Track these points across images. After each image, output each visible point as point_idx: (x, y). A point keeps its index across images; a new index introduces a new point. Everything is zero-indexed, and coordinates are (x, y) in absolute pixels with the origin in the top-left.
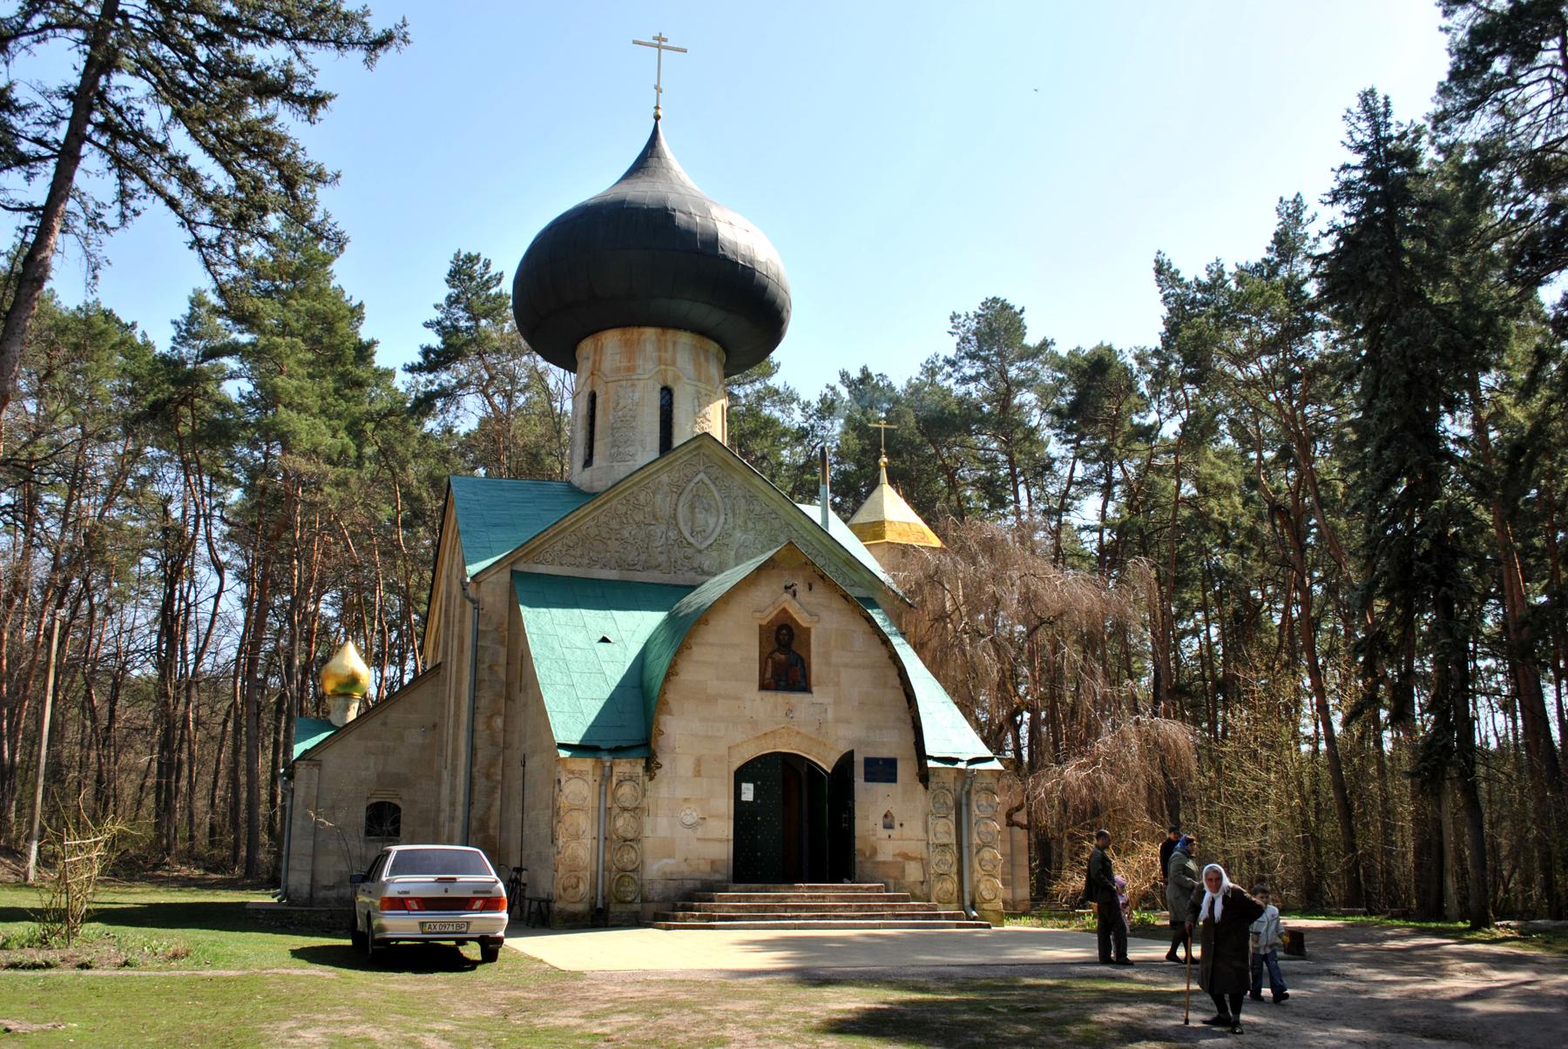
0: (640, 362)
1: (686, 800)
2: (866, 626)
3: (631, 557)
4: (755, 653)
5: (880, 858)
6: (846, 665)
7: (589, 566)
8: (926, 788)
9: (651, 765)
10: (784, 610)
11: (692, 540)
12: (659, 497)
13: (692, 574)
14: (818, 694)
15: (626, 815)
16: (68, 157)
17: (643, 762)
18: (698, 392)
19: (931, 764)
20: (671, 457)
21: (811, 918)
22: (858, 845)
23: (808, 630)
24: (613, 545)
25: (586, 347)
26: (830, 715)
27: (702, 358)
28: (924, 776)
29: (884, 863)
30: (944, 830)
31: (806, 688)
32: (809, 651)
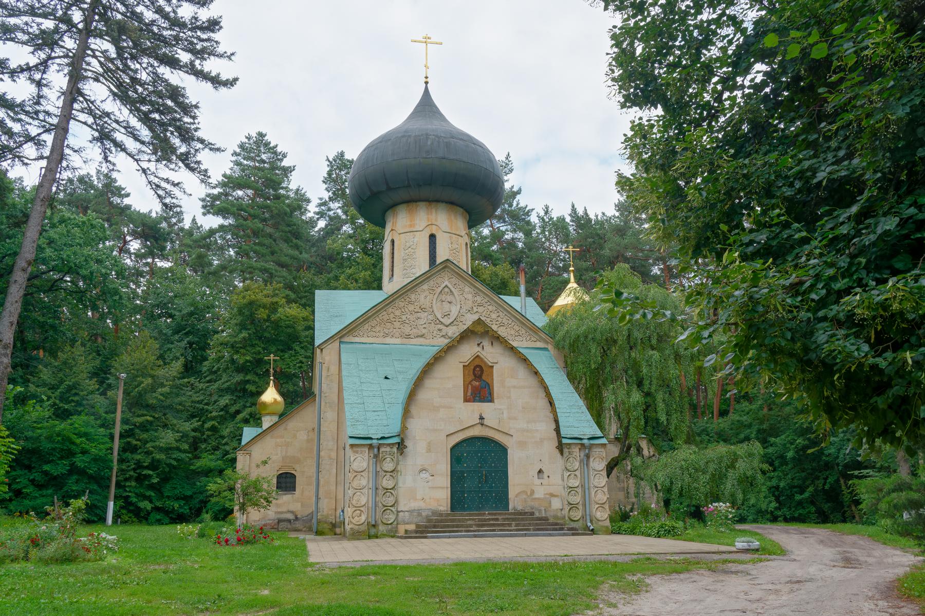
3: (407, 329)
4: (460, 382)
5: (536, 496)
6: (514, 387)
9: (401, 446)
12: (422, 297)
13: (442, 339)
14: (498, 404)
16: (61, 131)
19: (564, 441)
24: (397, 324)
26: (505, 415)
27: (453, 217)
29: (539, 499)
31: (491, 400)
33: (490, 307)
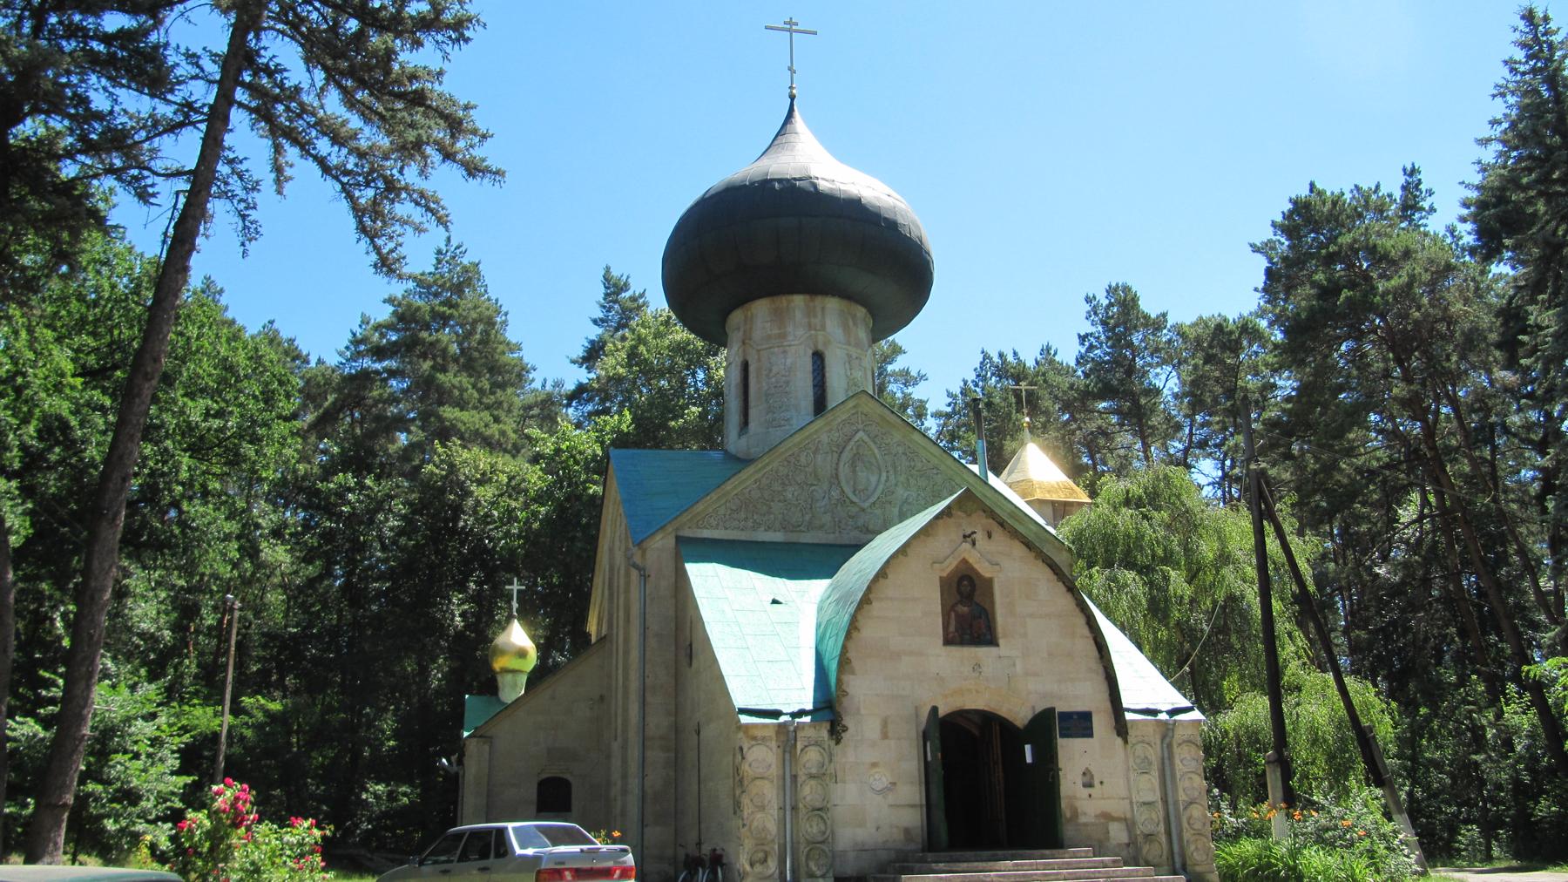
0: (790, 329)
1: (874, 765)
5: (1083, 819)
6: (1031, 616)
7: (754, 529)
8: (1126, 742)
9: (836, 729)
10: (964, 561)
11: (854, 499)
13: (856, 533)
14: (1005, 647)
15: (813, 782)
16: (217, 119)
17: (828, 726)
18: (849, 356)
20: (829, 416)
22: (1063, 805)
23: (990, 581)
25: (736, 317)
29: (1085, 825)
30: (1148, 788)
31: (992, 641)
32: (992, 603)
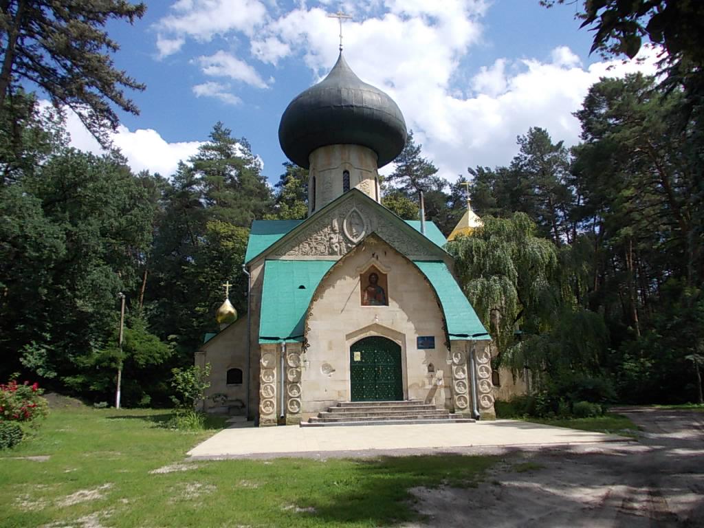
2: (416, 272)
3: (322, 248)
9: (304, 344)
10: (373, 266)
11: (351, 239)
18: (361, 173)
21: (379, 419)
23: (386, 275)
28: (448, 344)
32: (387, 285)
33: (393, 228)
